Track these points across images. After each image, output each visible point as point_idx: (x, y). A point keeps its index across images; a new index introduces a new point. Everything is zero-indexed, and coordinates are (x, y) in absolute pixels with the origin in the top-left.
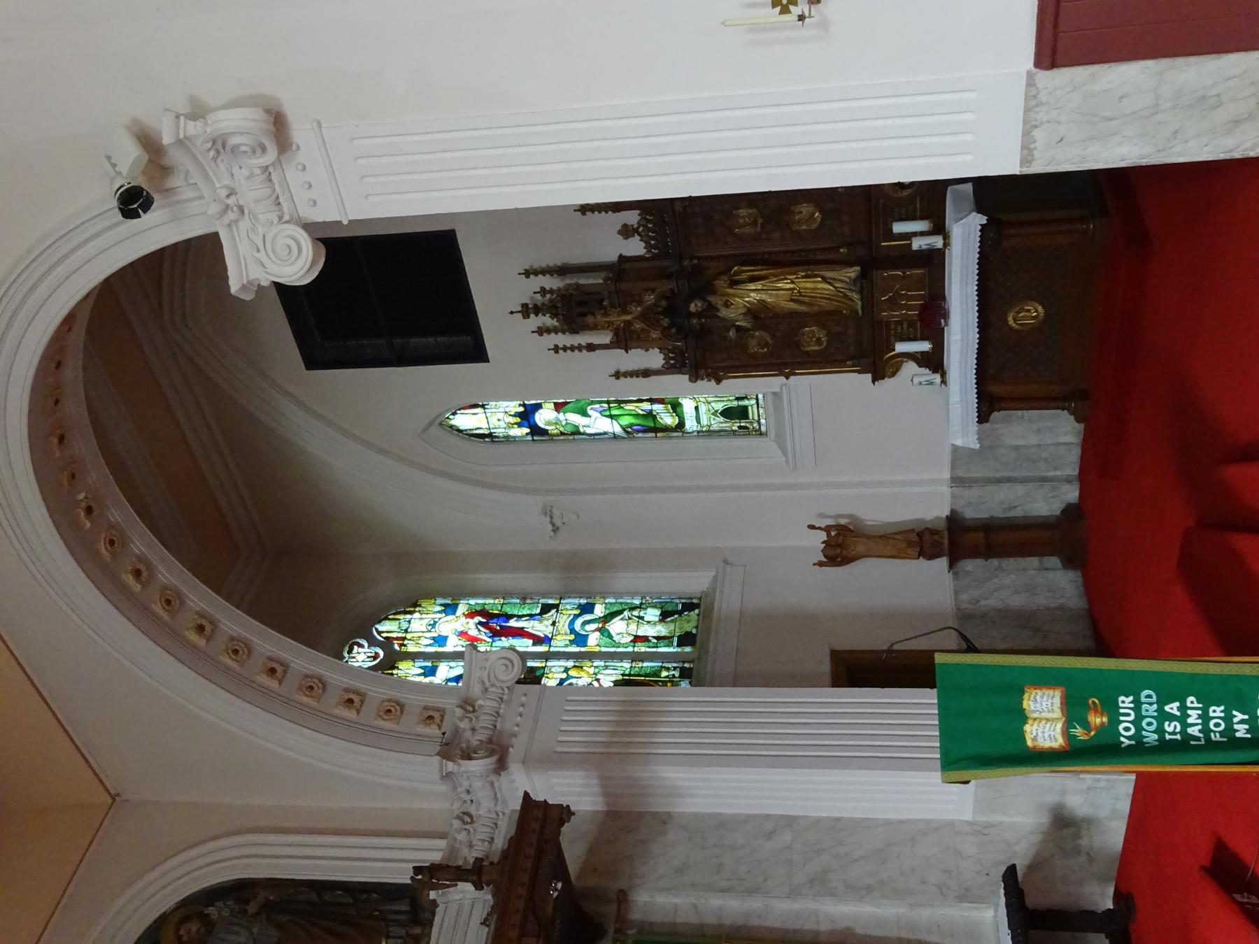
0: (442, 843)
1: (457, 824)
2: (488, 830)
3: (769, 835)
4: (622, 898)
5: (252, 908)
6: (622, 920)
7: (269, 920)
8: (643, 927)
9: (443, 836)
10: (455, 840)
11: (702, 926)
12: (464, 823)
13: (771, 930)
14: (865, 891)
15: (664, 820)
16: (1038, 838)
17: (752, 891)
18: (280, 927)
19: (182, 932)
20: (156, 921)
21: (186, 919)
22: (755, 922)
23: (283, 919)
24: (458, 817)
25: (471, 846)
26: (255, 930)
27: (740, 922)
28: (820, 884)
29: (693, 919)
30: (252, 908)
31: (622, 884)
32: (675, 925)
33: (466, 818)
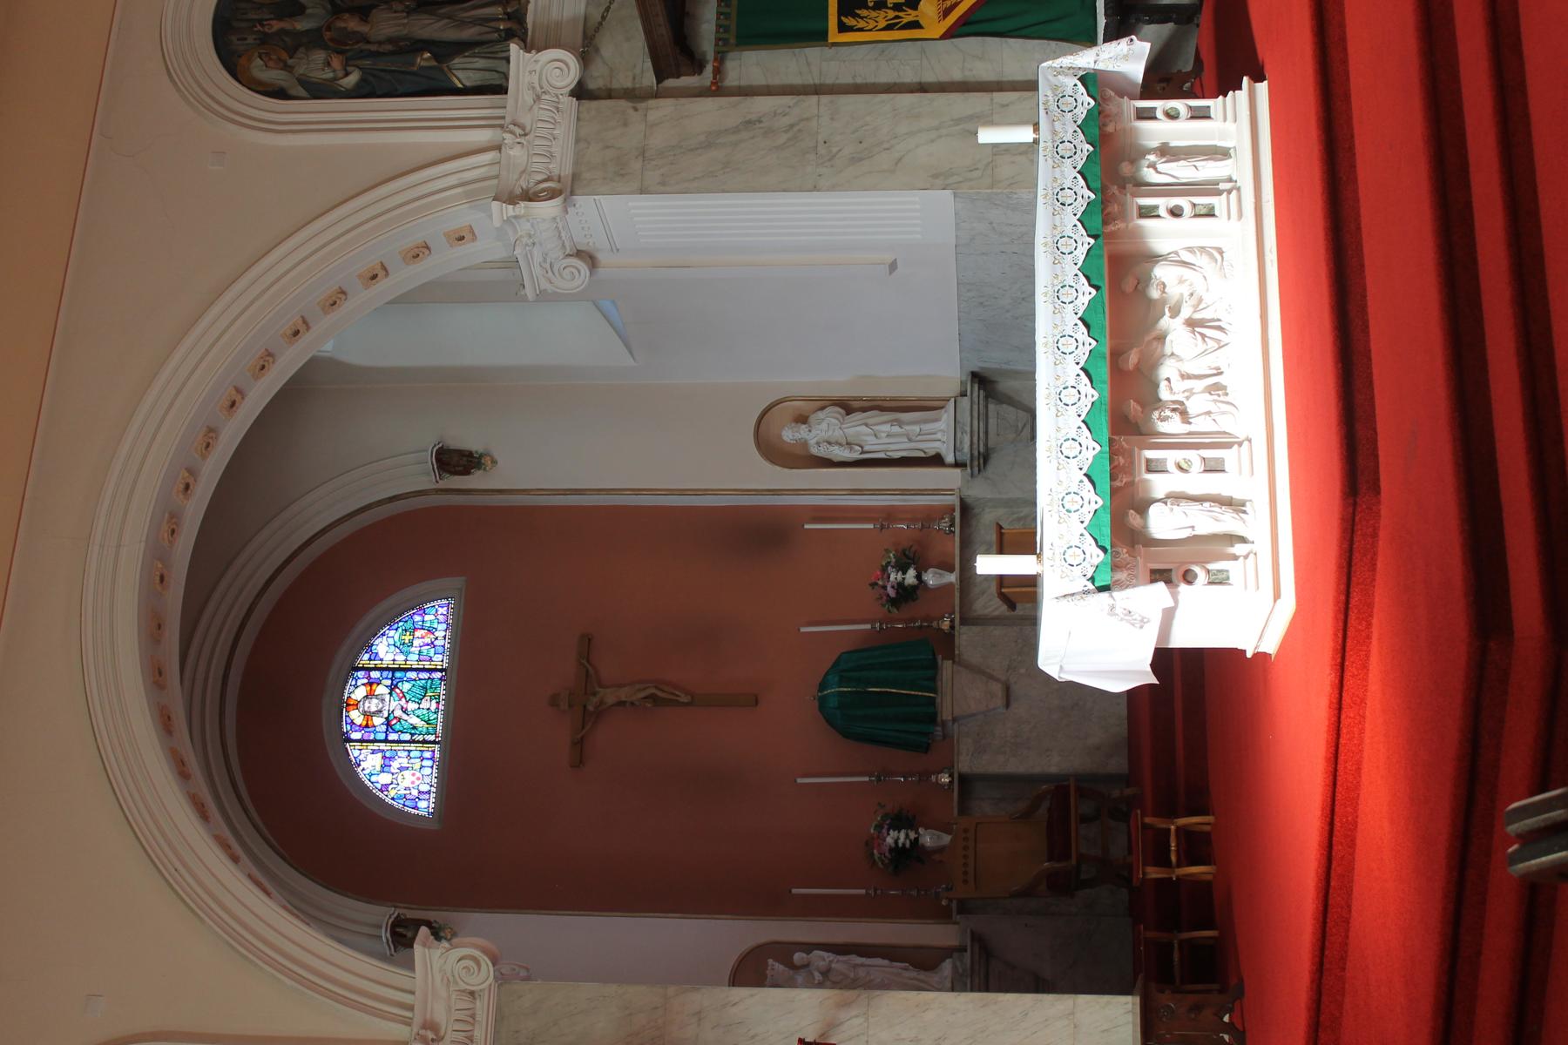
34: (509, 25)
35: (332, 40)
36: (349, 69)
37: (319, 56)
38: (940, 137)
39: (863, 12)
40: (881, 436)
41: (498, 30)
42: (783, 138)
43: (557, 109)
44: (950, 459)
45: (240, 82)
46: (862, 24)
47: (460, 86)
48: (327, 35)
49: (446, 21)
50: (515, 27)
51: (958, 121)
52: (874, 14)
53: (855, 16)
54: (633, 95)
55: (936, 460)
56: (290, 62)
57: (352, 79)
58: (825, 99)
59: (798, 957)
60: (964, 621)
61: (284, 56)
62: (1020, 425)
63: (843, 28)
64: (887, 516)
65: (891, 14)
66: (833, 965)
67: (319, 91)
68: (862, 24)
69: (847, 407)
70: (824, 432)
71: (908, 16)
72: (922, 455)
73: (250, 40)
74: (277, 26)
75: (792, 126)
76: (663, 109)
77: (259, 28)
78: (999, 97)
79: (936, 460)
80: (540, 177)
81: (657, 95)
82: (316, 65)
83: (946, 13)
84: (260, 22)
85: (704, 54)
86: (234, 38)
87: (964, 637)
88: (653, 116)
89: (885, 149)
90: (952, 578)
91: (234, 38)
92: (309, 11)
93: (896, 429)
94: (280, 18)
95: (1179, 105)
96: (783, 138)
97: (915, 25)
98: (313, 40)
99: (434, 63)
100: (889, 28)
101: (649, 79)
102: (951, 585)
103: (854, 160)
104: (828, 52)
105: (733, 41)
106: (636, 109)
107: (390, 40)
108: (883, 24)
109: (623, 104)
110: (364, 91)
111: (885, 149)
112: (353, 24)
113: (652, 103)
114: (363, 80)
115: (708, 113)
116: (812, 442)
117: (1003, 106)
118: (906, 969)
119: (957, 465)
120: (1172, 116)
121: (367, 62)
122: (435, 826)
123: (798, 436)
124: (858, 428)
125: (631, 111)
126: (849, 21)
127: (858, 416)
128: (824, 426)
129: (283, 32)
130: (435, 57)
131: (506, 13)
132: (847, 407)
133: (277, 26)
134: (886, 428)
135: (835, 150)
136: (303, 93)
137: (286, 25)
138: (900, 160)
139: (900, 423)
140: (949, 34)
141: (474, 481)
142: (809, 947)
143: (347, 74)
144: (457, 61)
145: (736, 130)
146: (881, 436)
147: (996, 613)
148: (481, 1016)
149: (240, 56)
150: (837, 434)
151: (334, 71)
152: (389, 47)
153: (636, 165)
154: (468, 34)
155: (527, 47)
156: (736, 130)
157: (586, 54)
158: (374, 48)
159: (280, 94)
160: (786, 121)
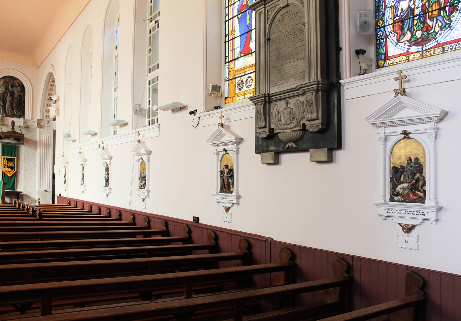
0: (31, 119)
2: (33, 125)
3: (33, 164)
4: (23, 144)
5: (20, 93)
6: (20, 144)
7: (18, 96)
8: (20, 146)
9: (32, 119)
11: (20, 154)
13: (20, 163)
14: (25, 176)
16: (34, 198)
17: (24, 162)
18: (17, 97)
19: (16, 84)
20: (18, 79)
21: (18, 83)
22: (21, 161)
23: (18, 98)
25: (30, 123)
26: (17, 94)
27: (21, 159)
28: (26, 170)
29: (21, 153)
30: (20, 93)
31: (25, 144)
32: (20, 151)
34: (8, 115)
35: (7, 92)
39: (7, 161)
41: (7, 113)
46: (5, 161)
48: (7, 91)
49: (8, 106)
50: (8, 116)
52: (6, 162)
53: (6, 160)
56: (4, 86)
61: (5, 85)
63: (4, 158)
65: (6, 164)
68: (5, 161)
71: (6, 167)
73: (8, 81)
74: (10, 84)
77: (10, 82)
83: (6, 171)
84: (11, 82)
85: (2, 140)
86: (8, 78)
91: (8, 78)
92: (12, 89)
94: (11, 85)
97: (4, 167)
98: (7, 89)
99: (1, 105)
100: (4, 164)
104: (1, 156)
105: (3, 144)
107: (6, 99)
108: (5, 163)
112: (9, 95)
121: (2, 96)
126: (5, 159)
129: (9, 85)
131: (10, 115)
133: (10, 84)
137: (10, 85)
140: (3, 172)
149: (5, 79)
152: (4, 99)
154: (6, 110)
158: (5, 97)
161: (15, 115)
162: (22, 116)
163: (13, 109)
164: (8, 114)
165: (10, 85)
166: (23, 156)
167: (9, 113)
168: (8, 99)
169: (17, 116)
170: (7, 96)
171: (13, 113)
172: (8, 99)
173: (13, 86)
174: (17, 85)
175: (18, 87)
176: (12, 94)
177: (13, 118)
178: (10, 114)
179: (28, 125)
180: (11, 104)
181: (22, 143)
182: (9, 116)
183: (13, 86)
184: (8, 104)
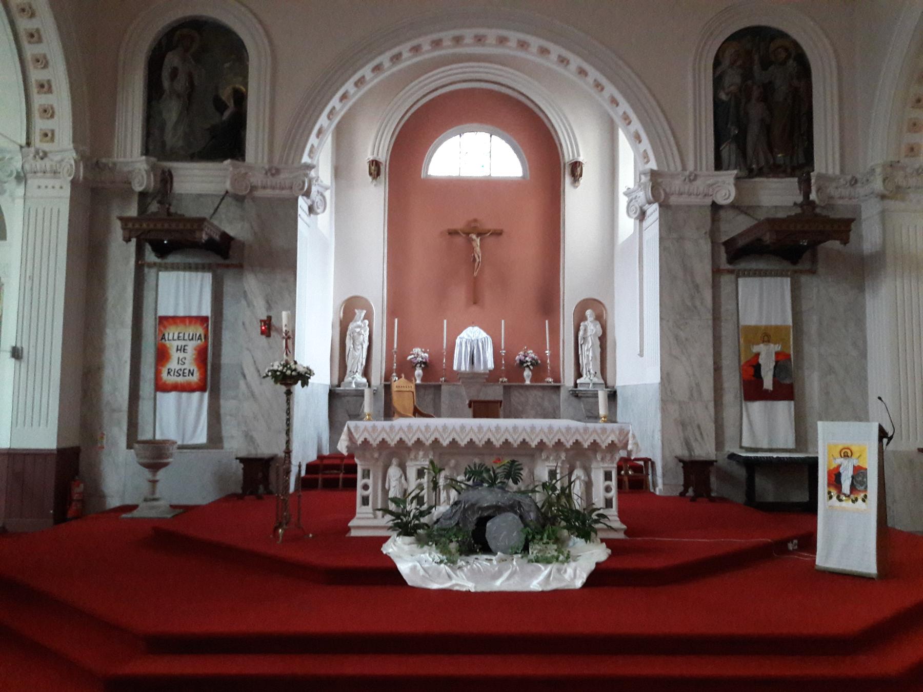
0: (838, 172)
1: (849, 177)
3: (854, 344)
4: (813, 272)
9: (842, 171)
10: (840, 179)
12: (851, 181)
15: (861, 289)
24: (853, 177)
31: (821, 269)
33: (854, 182)
36: (730, 96)
37: (738, 80)
38: (690, 377)
40: (589, 353)
41: (751, 165)
42: (689, 304)
43: (705, 195)
44: (578, 381)
45: (724, 43)
47: (721, 149)
51: (698, 385)
54: (713, 235)
55: (579, 375)
57: (723, 96)
58: (710, 322)
59: (367, 322)
60: (505, 387)
61: (739, 63)
62: (592, 412)
64: (556, 355)
66: (362, 336)
67: (718, 82)
69: (603, 339)
70: (591, 328)
72: (581, 369)
74: (756, 57)
75: (695, 307)
76: (706, 247)
78: (711, 405)
79: (579, 375)
80: (668, 190)
81: (714, 243)
82: (733, 79)
87: (498, 387)
88: (702, 242)
89: (682, 351)
90: (528, 382)
93: (590, 358)
95: (613, 493)
96: (689, 304)
98: (747, 75)
101: (724, 238)
102: (524, 380)
103: (677, 338)
106: (706, 233)
109: (708, 228)
110: (717, 103)
111: (682, 351)
112: (756, 93)
113: (709, 241)
114: (723, 102)
115: (703, 269)
116: (586, 323)
117: (707, 408)
118: (362, 365)
119: (576, 385)
120: (608, 489)
122: (423, 176)
123: (588, 317)
124: (590, 342)
125: (704, 232)
127: (598, 343)
128: (592, 327)
130: (737, 136)
132: (603, 339)
133: (756, 57)
134: (591, 355)
135: (682, 327)
136: (718, 73)
137: (756, 62)
138: (677, 358)
139: (594, 357)
141: (568, 180)
142: (370, 326)
143: (727, 94)
144: (733, 146)
145: (693, 282)
146: (589, 353)
147: (512, 400)
148: (284, 192)
150: (589, 334)
151: (729, 87)
153: (675, 235)
155: (738, 178)
156: (693, 282)
157: (734, 206)
159: (717, 63)
160: (698, 303)
161: (779, 166)
162: (801, 167)
163: (771, 148)
164: (754, 166)
165: (756, 62)
166: (815, 318)
167: (758, 164)
168: (756, 111)
169: (785, 172)
170: (749, 99)
171: (771, 162)
172: (756, 111)
173: (766, 64)
174: (783, 55)
175: (784, 63)
176: (768, 90)
177: (774, 177)
178: (762, 163)
179: (831, 198)
180: (767, 129)
181: (807, 266)
182: (761, 173)
183: (766, 64)
184: (754, 130)
